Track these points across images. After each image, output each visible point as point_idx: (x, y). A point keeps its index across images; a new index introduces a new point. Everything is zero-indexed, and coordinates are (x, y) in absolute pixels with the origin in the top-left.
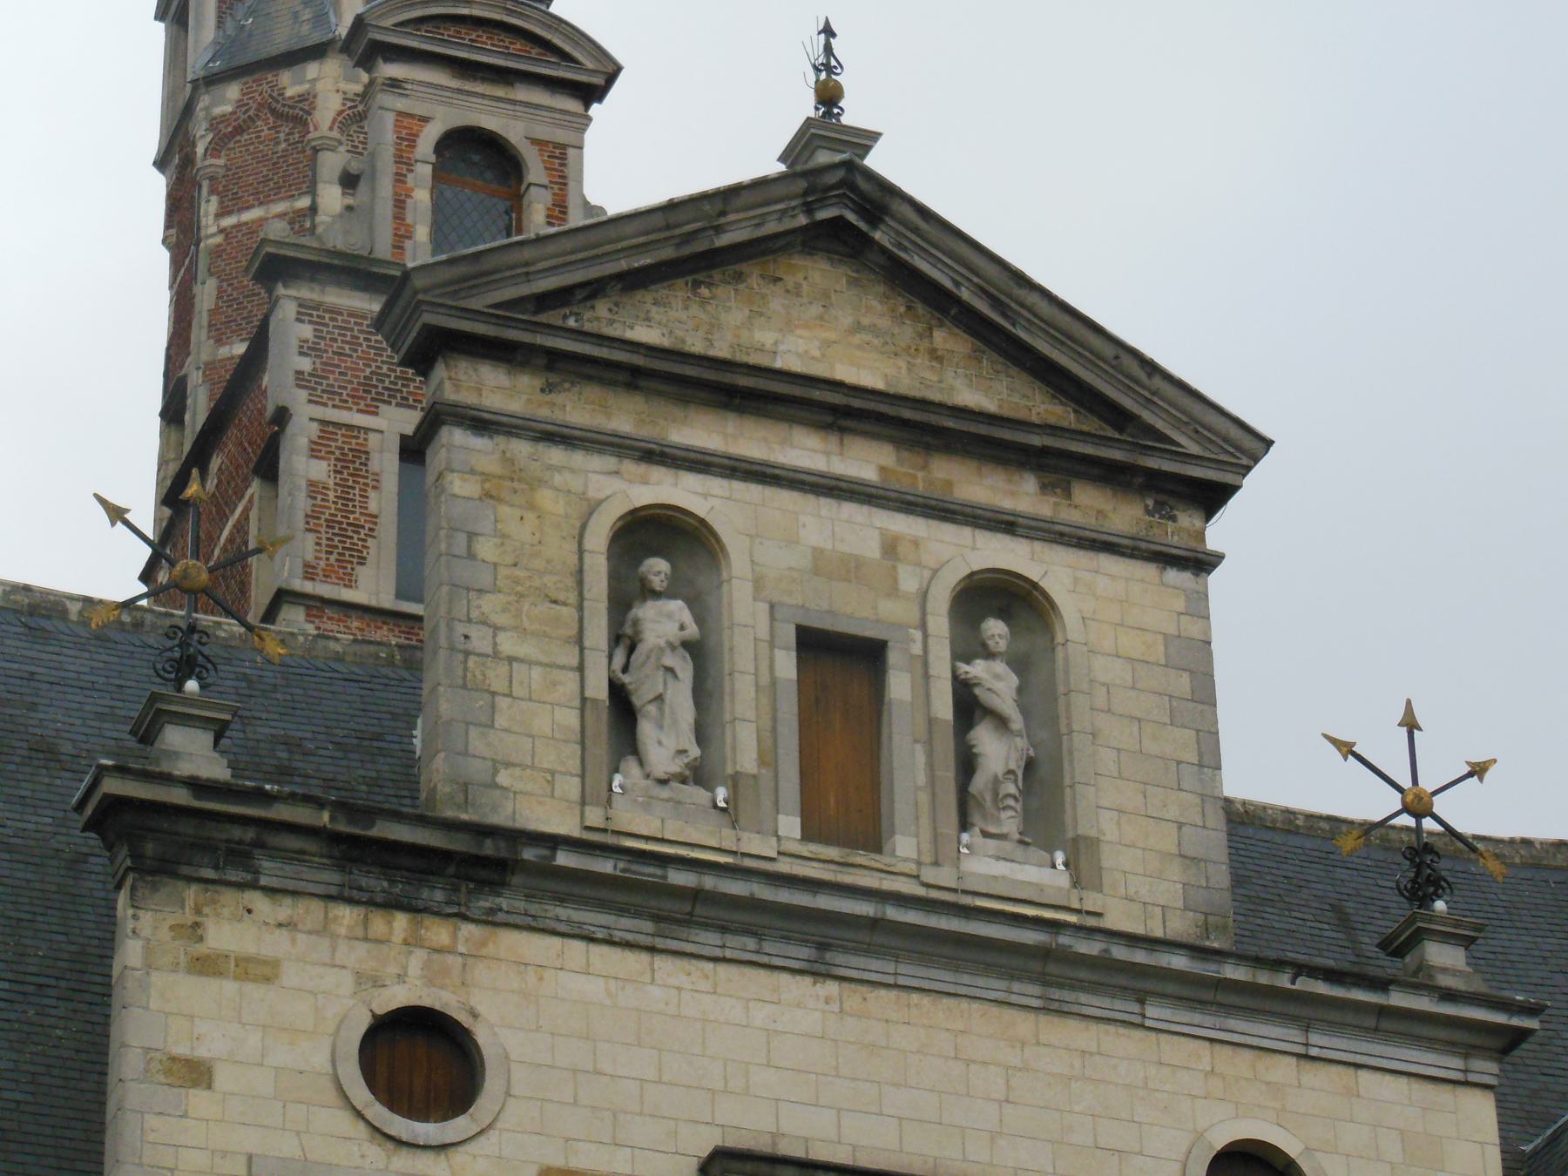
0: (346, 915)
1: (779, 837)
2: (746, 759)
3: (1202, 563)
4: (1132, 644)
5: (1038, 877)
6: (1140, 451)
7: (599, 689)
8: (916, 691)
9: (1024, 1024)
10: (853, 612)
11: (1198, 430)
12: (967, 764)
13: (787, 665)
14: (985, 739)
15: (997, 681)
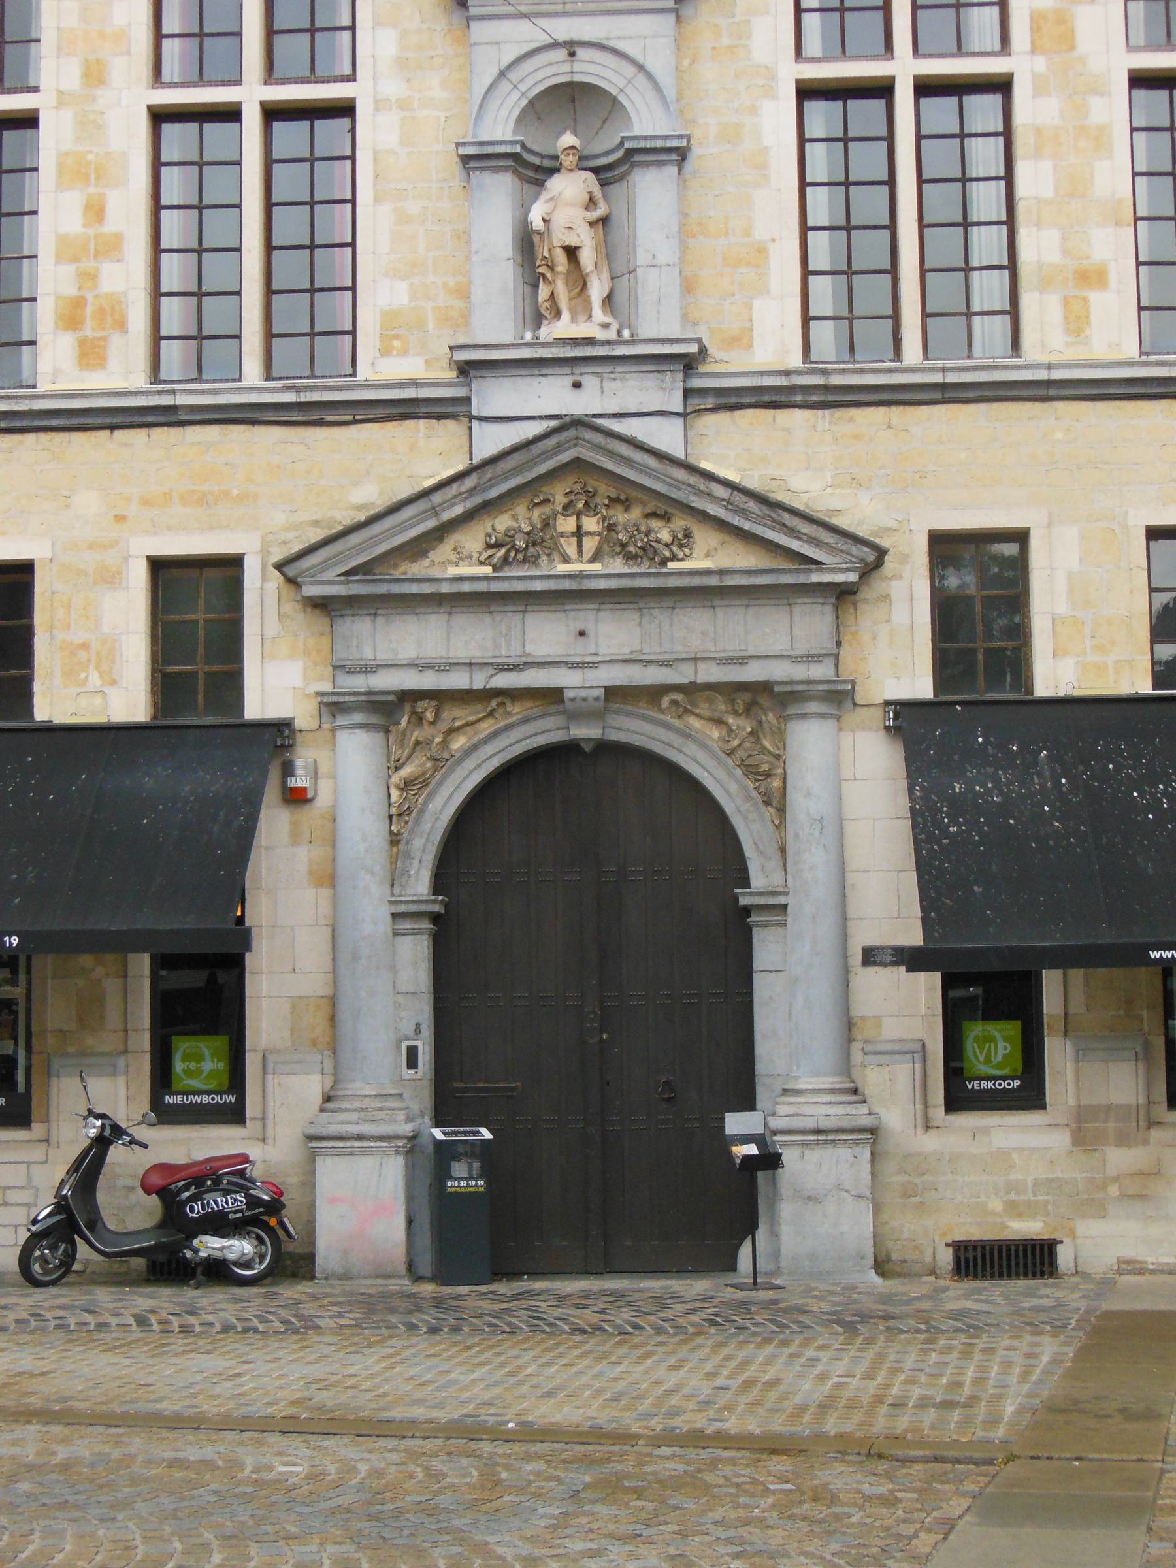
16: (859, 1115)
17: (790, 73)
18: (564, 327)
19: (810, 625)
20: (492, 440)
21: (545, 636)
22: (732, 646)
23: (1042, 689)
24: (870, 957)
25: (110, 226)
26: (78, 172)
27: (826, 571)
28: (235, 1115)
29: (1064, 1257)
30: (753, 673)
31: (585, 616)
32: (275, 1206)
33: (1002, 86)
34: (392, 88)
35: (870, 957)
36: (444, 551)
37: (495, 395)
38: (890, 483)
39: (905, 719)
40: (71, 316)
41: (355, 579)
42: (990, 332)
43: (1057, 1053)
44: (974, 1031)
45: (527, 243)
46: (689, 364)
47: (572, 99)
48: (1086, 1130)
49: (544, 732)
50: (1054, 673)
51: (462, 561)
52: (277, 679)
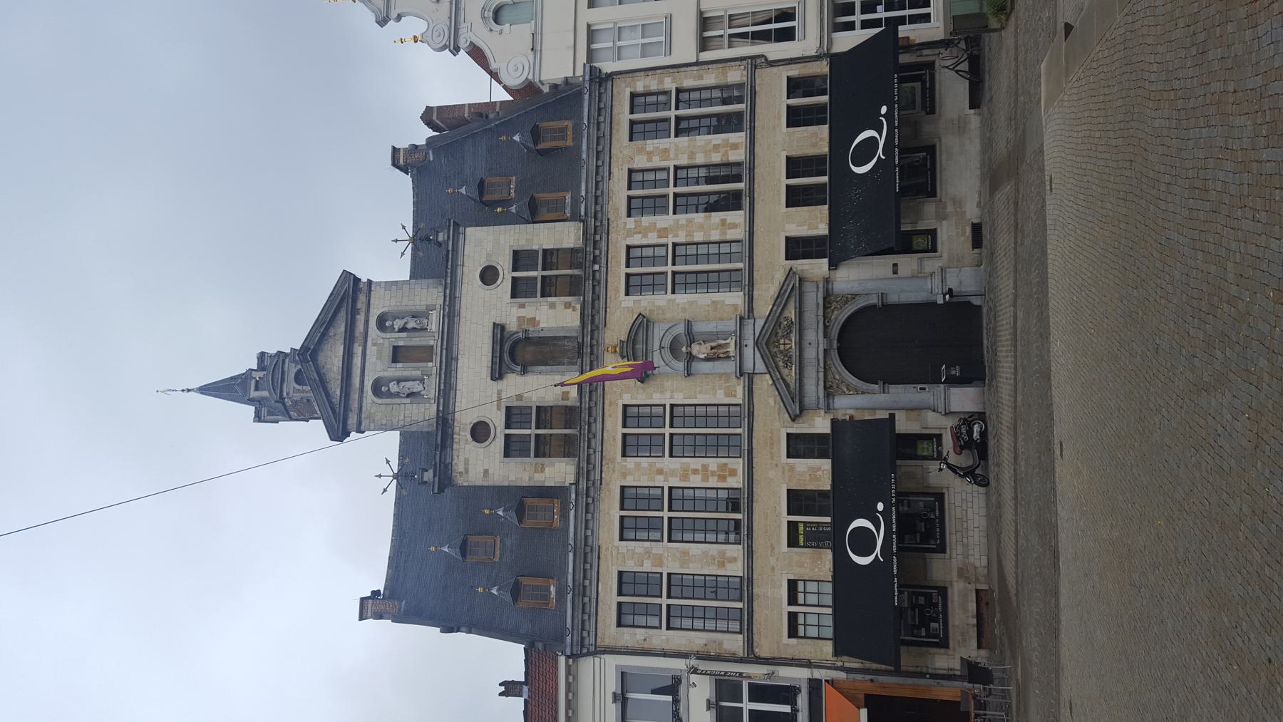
0: (455, 446)
1: (433, 367)
2: (419, 373)
3: (370, 282)
4: (387, 297)
5: (434, 316)
6: (350, 294)
7: (408, 400)
8: (402, 340)
9: (462, 320)
10: (388, 352)
11: (342, 286)
12: (414, 329)
13: (400, 365)
14: (409, 326)
15: (398, 324)
16: (937, 271)
17: (670, 296)
18: (731, 349)
19: (809, 288)
20: (761, 367)
21: (810, 353)
22: (814, 306)
23: (826, 232)
24: (895, 272)
25: (700, 467)
26: (685, 477)
27: (793, 288)
28: (939, 437)
29: (976, 221)
30: (821, 301)
31: (805, 343)
32: (965, 420)
33: (675, 245)
34: (668, 395)
35: (895, 272)
36: (788, 379)
37: (748, 366)
38: (773, 267)
39: (833, 265)
40: (722, 478)
41: (796, 405)
42: (735, 248)
43: (922, 226)
44: (915, 247)
45: (708, 359)
46: (742, 318)
47: (674, 349)
48: (942, 217)
49: (834, 354)
50: (823, 229)
51: (791, 374)
52: (821, 424)
